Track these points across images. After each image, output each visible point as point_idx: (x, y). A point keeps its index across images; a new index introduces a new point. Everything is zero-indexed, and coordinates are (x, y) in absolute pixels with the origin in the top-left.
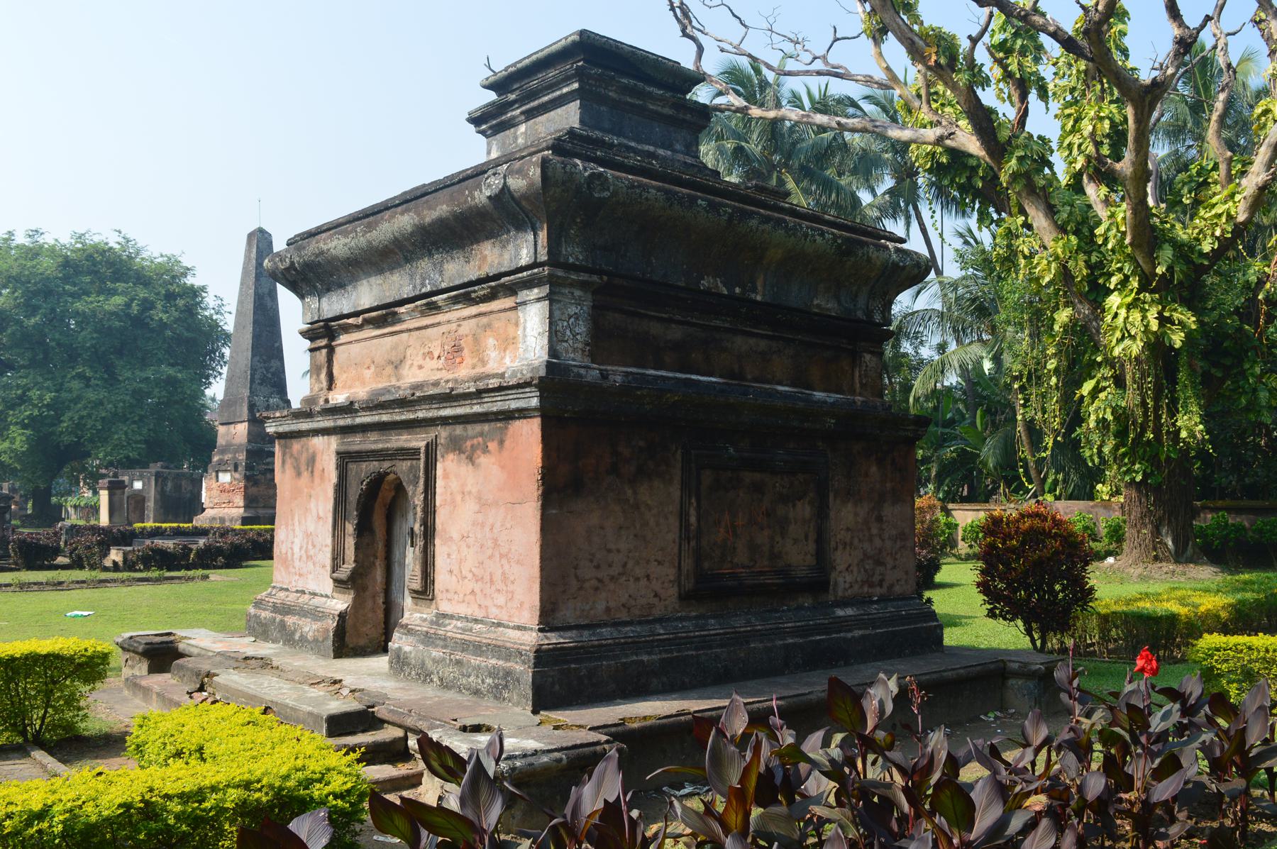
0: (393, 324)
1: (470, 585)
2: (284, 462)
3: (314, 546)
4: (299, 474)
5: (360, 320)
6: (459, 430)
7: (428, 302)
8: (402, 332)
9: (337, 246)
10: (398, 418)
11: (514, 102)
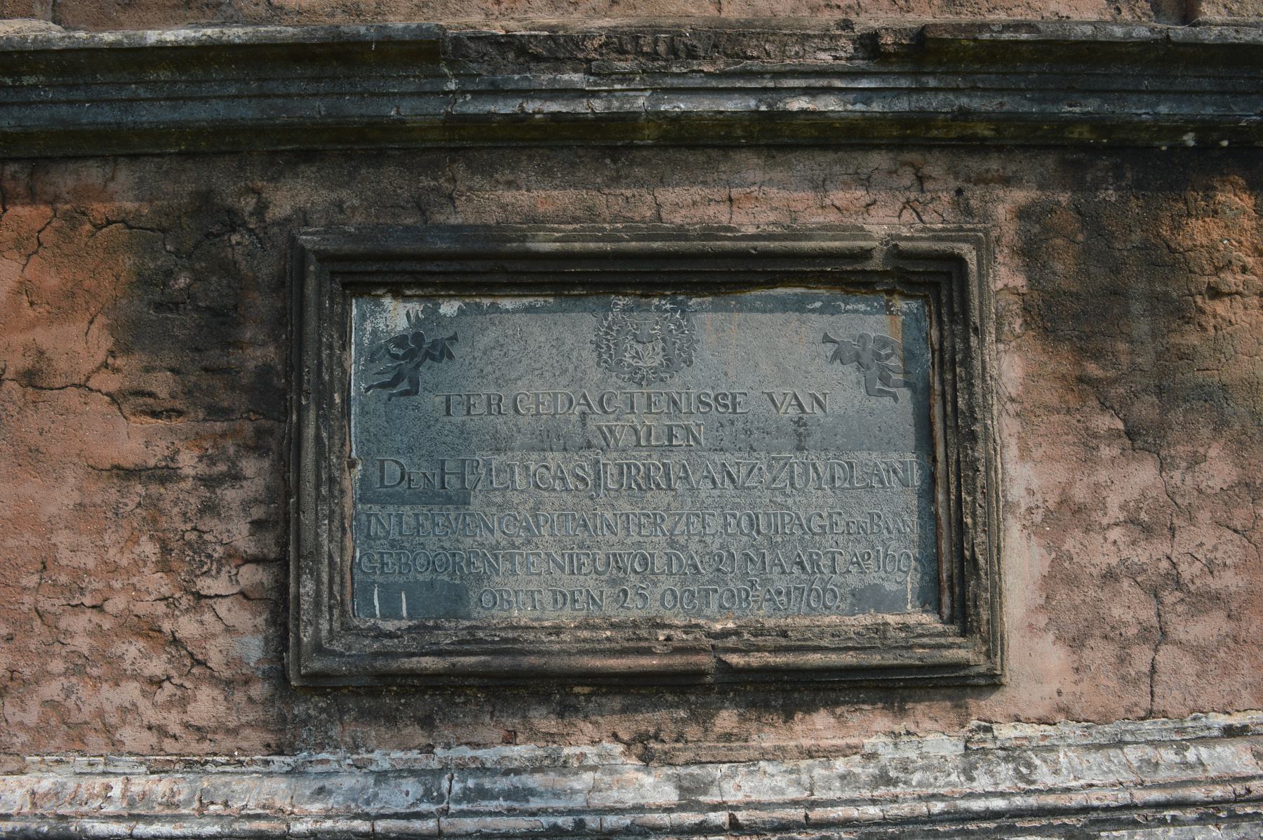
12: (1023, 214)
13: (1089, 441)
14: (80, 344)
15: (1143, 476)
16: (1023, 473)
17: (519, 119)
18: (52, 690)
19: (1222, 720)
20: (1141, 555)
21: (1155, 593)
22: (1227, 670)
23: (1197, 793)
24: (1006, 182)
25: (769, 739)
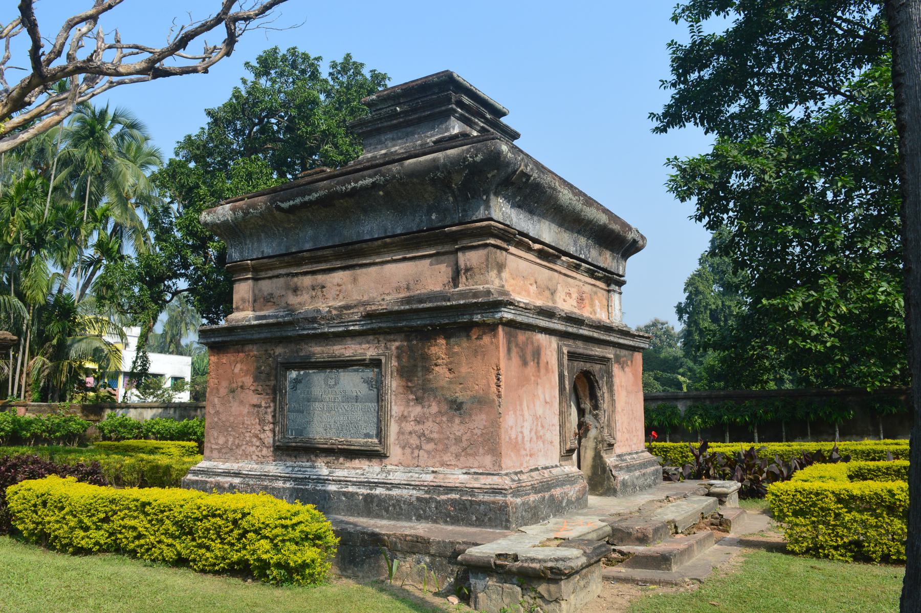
0: (549, 262)
1: (626, 436)
2: (509, 350)
3: (543, 427)
4: (525, 363)
5: (537, 246)
6: (624, 352)
7: (577, 264)
8: (556, 271)
9: (565, 196)
10: (602, 337)
11: (486, 118)
13: (408, 401)
14: (249, 380)
15: (417, 410)
16: (396, 408)
17: (308, 334)
18: (243, 447)
19: (432, 469)
20: (417, 428)
21: (419, 437)
22: (434, 457)
23: (413, 483)
24: (394, 341)
25: (348, 464)
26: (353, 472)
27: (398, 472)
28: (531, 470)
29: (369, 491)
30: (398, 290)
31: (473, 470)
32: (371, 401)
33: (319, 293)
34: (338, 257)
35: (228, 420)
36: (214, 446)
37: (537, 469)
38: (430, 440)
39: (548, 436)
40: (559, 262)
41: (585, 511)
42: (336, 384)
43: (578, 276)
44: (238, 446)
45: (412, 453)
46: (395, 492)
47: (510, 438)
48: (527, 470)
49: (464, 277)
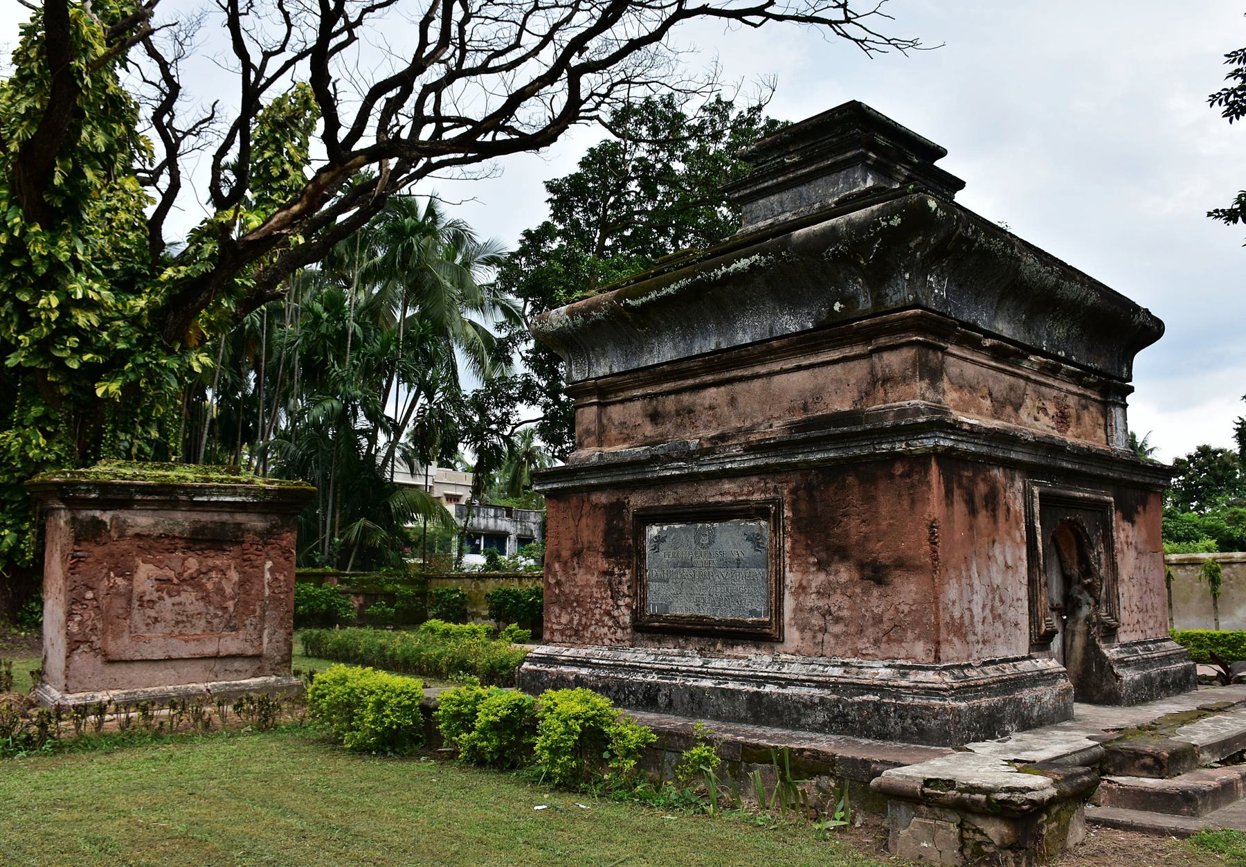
1: (1137, 616)
2: (949, 493)
3: (1002, 601)
4: (973, 512)
5: (988, 342)
12: (792, 492)
15: (822, 577)
18: (592, 628)
21: (824, 616)
22: (844, 643)
25: (728, 652)
26: (735, 662)
27: (791, 665)
28: (985, 664)
29: (755, 689)
30: (791, 410)
31: (898, 662)
32: (758, 566)
33: (686, 420)
34: (710, 369)
35: (572, 592)
36: (555, 627)
37: (992, 662)
38: (838, 620)
39: (1011, 614)
40: (1026, 364)
41: (1067, 724)
42: (710, 543)
43: (1056, 384)
44: (586, 627)
45: (814, 637)
46: (790, 691)
47: (952, 617)
48: (978, 663)
49: (882, 391)
